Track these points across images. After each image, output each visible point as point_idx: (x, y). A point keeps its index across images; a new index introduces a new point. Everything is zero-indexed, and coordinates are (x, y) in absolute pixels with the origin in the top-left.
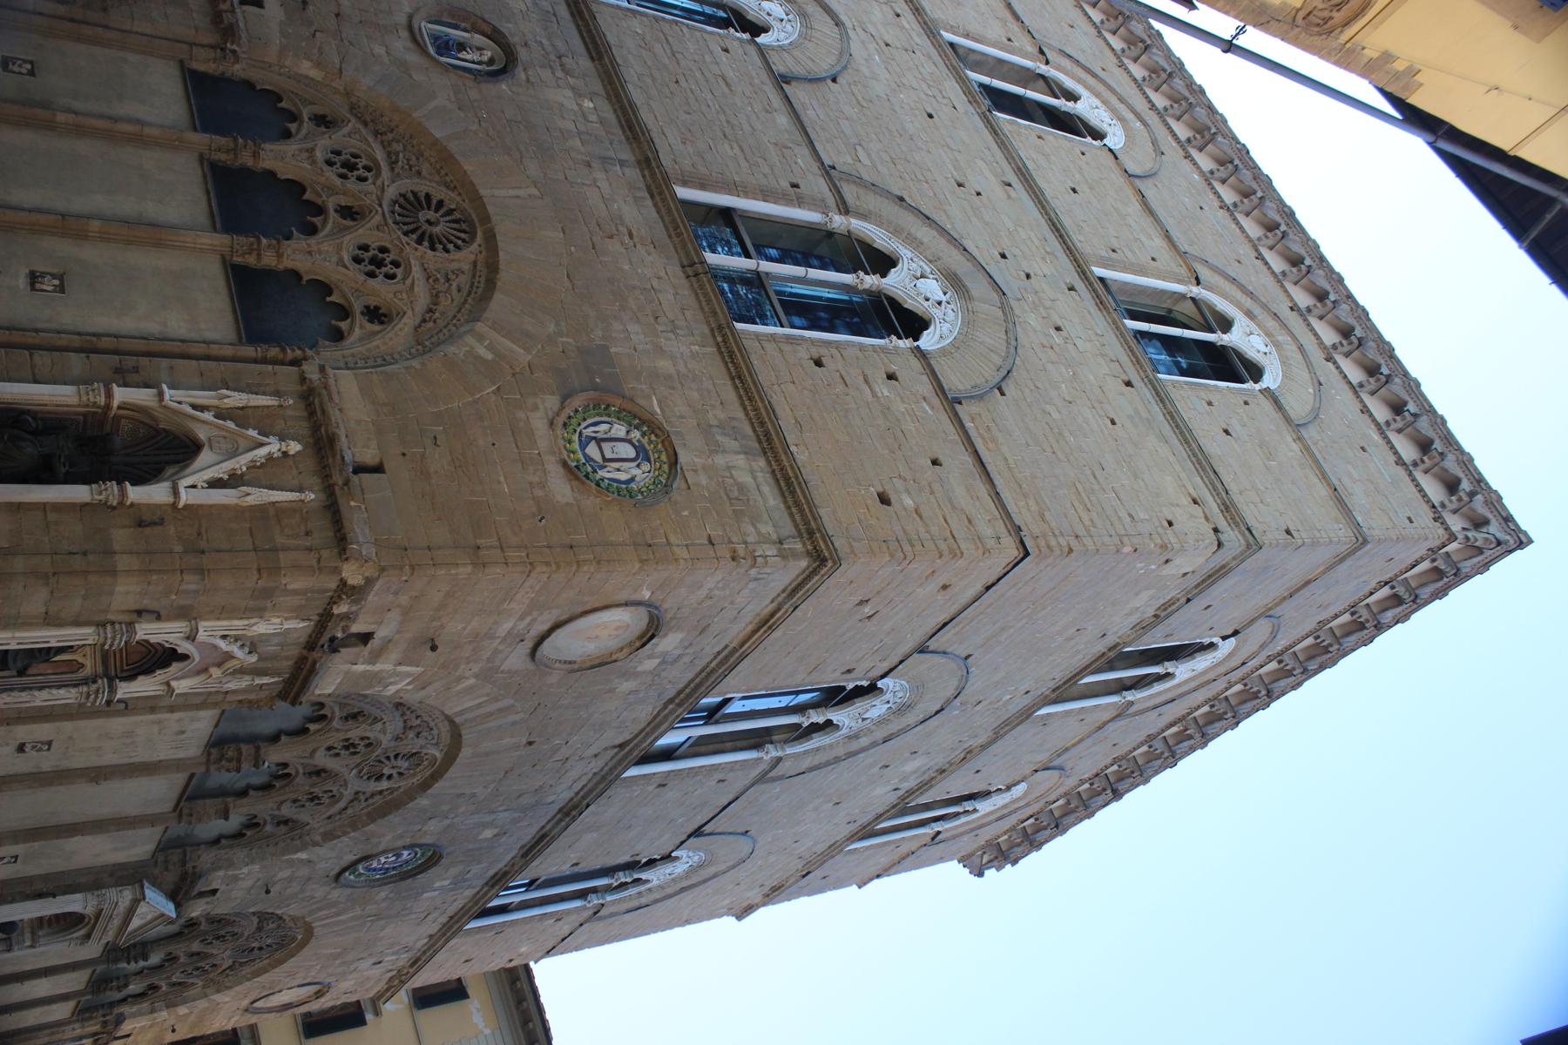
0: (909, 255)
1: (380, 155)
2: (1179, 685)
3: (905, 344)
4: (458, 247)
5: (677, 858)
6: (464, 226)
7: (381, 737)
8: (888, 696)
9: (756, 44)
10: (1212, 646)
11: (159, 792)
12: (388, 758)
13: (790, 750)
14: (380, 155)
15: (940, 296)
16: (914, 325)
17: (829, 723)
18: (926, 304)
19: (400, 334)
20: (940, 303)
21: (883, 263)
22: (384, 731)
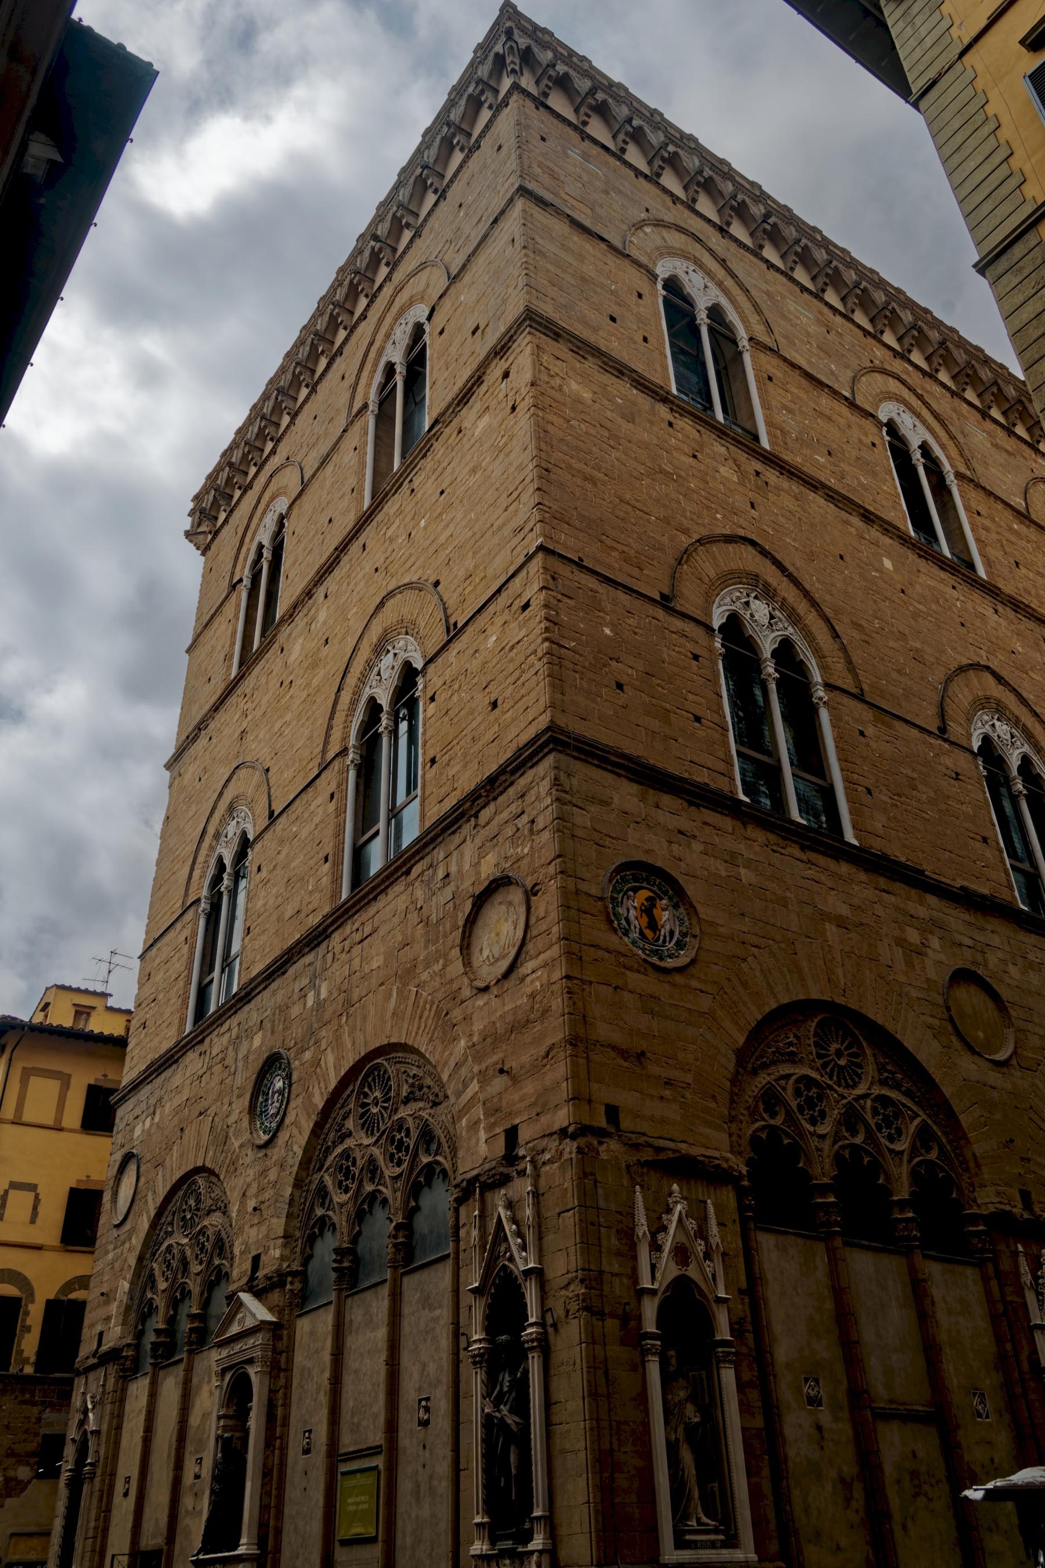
0: (367, 689)
1: (339, 1150)
2: (726, 292)
3: (420, 681)
4: (389, 1079)
5: (986, 739)
6: (376, 1073)
7: (794, 1078)
8: (738, 607)
9: (255, 840)
10: (672, 285)
11: (870, 1271)
12: (824, 1066)
13: (817, 677)
14: (339, 1150)
15: (391, 655)
16: (409, 675)
17: (775, 654)
18: (396, 668)
19: (438, 1119)
20: (395, 654)
21: (374, 708)
22: (787, 1077)
